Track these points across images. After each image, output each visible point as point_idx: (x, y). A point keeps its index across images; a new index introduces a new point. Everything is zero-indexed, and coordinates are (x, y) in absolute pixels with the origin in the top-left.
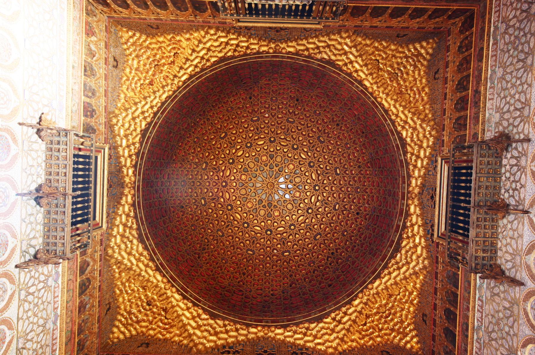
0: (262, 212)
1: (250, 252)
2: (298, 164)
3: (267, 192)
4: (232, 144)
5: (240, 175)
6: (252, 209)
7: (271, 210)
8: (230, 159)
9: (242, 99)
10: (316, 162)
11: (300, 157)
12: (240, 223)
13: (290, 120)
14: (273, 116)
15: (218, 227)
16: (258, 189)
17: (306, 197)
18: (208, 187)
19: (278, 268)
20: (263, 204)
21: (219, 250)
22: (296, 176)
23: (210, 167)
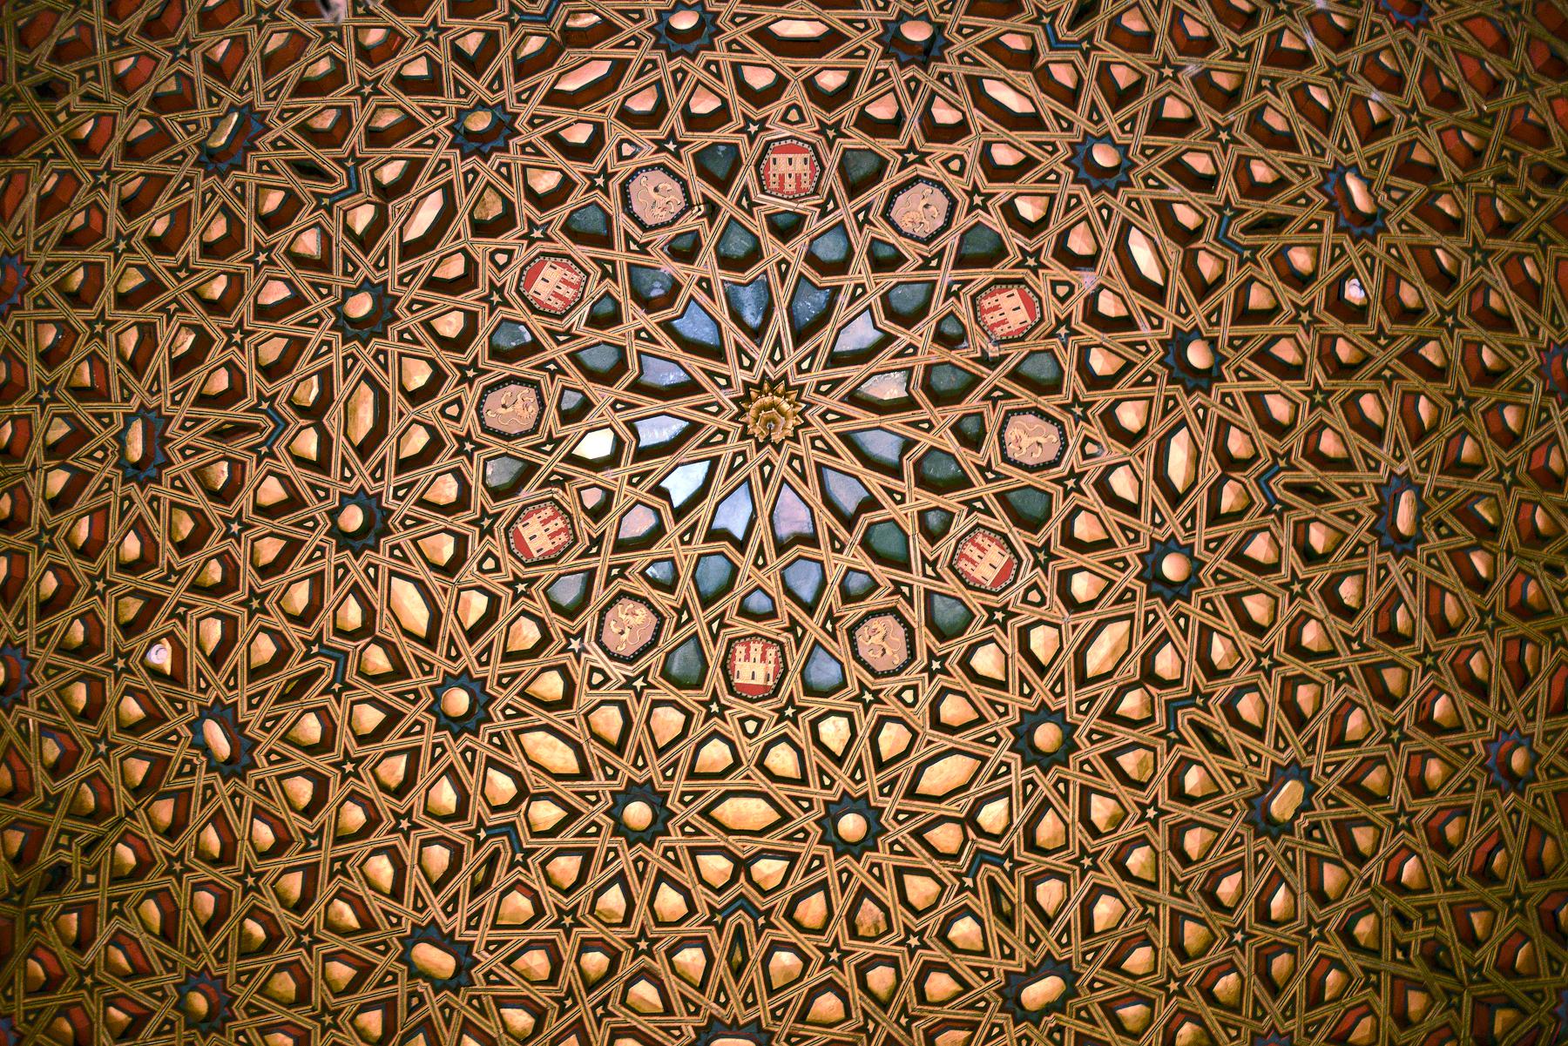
0: (1030, 439)
1: (1404, 519)
2: (508, 239)
3: (830, 432)
4: (496, 846)
5: (740, 708)
6: (1018, 537)
7: (992, 363)
8: (620, 829)
9: (81, 944)
10: (449, 101)
11: (446, 244)
12: (1166, 622)
13: (136, 451)
14: (153, 603)
15: (1233, 825)
16: (826, 518)
17: (795, 93)
18: (910, 969)
19: (1496, 276)
20: (952, 444)
21: (1426, 808)
22: (622, 222)
23: (735, 992)
